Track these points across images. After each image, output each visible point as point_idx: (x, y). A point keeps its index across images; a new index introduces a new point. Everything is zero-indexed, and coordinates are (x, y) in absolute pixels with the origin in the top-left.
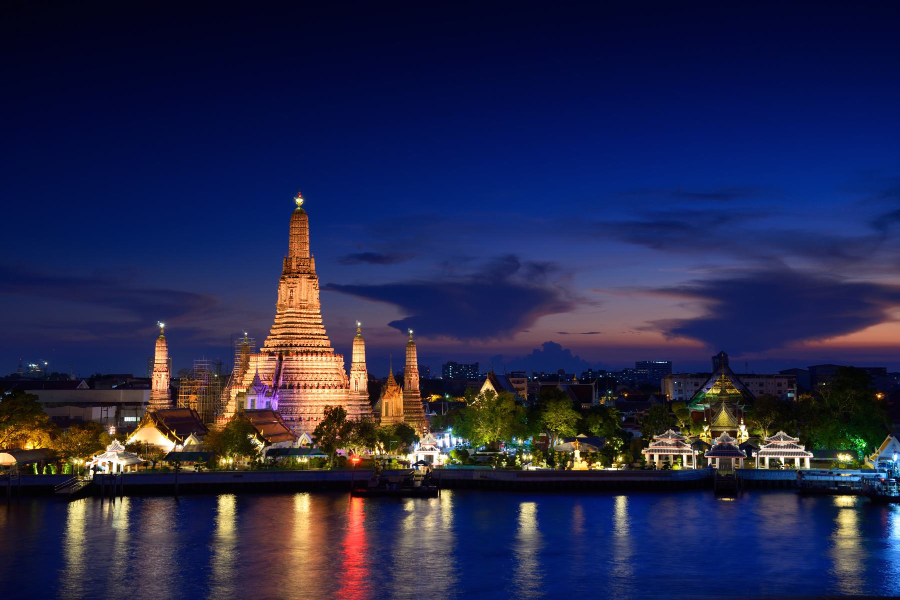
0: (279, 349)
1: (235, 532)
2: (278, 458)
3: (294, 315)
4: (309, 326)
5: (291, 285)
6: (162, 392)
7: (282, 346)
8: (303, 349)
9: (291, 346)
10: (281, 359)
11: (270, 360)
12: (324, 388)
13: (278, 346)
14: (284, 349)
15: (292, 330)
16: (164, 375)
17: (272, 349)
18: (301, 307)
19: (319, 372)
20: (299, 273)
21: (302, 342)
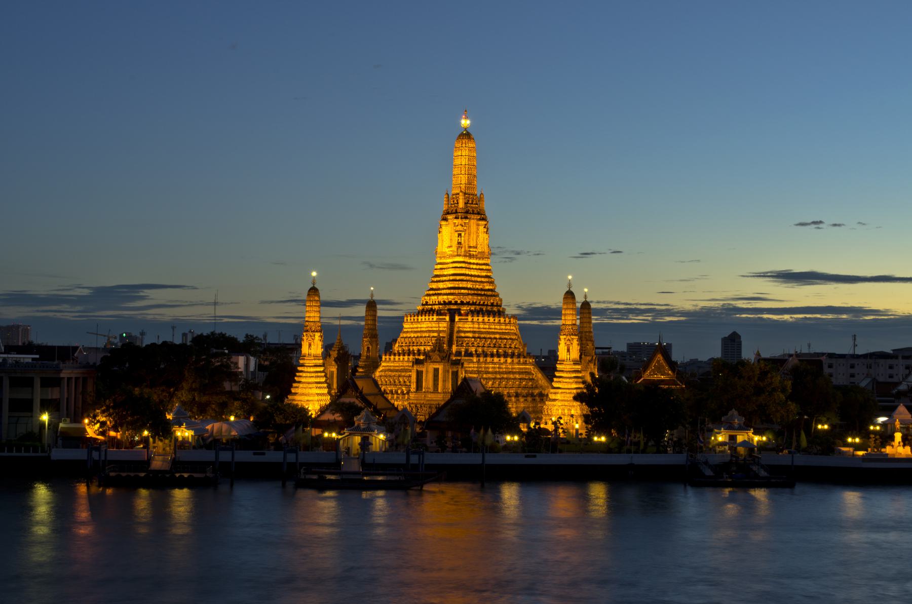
0: (448, 307)
1: (607, 514)
2: (898, 426)
3: (463, 265)
4: (479, 279)
5: (459, 228)
6: (316, 357)
7: (450, 303)
8: (478, 308)
9: (462, 303)
10: (452, 320)
11: (438, 321)
12: (506, 355)
13: (445, 303)
14: (455, 307)
15: (456, 284)
16: (317, 335)
17: (436, 307)
18: (471, 256)
19: (498, 336)
20: (467, 212)
21: (475, 299)
